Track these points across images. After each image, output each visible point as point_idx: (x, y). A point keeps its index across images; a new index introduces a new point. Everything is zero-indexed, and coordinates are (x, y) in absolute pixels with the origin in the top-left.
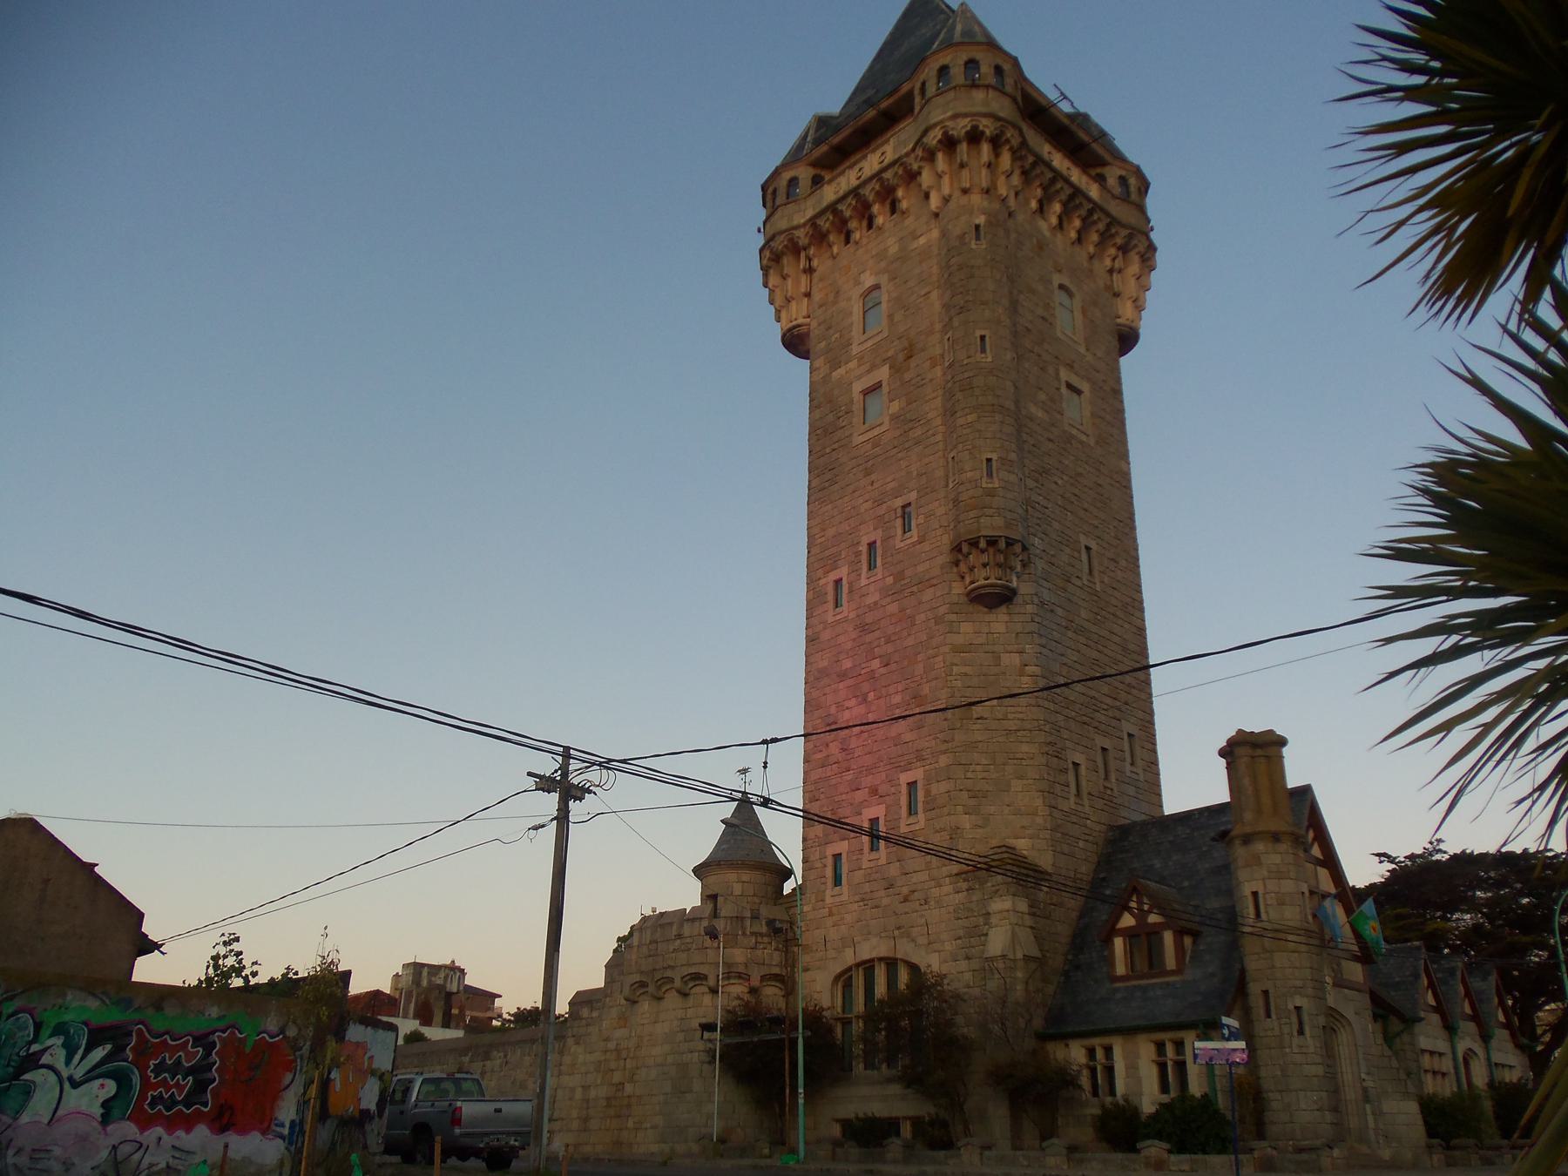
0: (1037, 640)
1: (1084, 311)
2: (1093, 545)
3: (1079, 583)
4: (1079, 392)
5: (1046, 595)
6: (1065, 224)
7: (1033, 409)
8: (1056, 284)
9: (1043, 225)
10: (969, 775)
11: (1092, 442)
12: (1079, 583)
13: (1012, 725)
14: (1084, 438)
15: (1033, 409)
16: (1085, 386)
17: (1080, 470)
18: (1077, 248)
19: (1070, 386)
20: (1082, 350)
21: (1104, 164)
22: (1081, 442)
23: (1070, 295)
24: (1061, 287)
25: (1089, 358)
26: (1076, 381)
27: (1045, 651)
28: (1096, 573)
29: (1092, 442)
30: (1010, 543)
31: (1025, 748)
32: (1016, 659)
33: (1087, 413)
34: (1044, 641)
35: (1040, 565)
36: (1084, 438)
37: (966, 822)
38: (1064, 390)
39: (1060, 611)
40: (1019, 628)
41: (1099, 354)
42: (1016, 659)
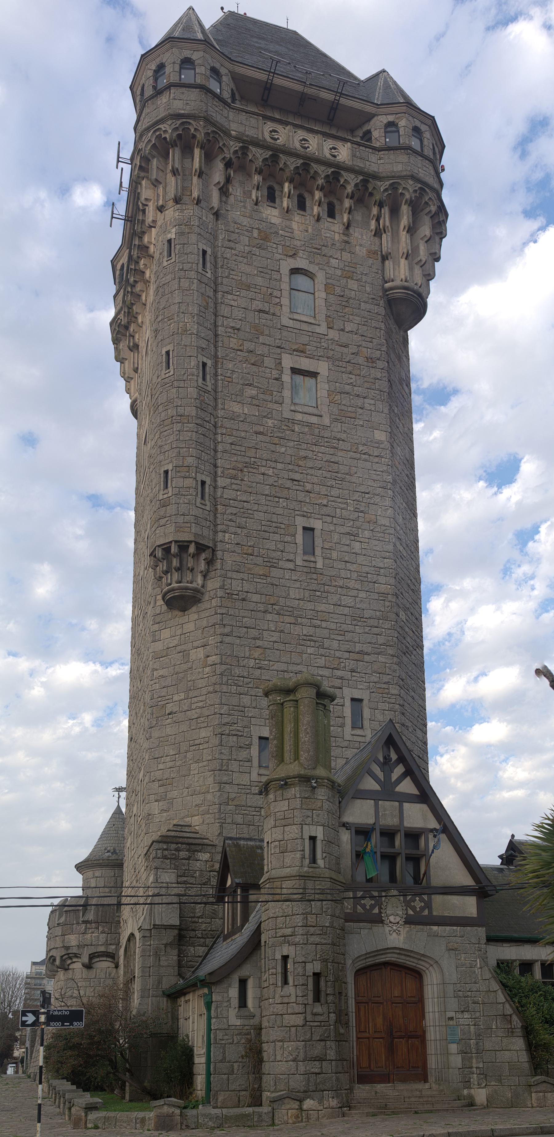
0: (219, 631)
1: (328, 288)
2: (317, 525)
3: (291, 565)
4: (314, 375)
5: (236, 586)
6: (308, 204)
7: (236, 408)
8: (285, 271)
9: (272, 214)
10: (161, 766)
11: (326, 421)
12: (291, 565)
13: (193, 714)
14: (314, 420)
15: (236, 408)
16: (322, 368)
17: (302, 453)
18: (327, 223)
19: (295, 371)
20: (322, 329)
21: (370, 117)
22: (310, 425)
23: (310, 275)
24: (295, 271)
25: (333, 334)
26: (305, 364)
27: (227, 639)
28: (318, 551)
29: (326, 421)
30: (183, 547)
31: (203, 733)
32: (201, 653)
33: (323, 393)
34: (227, 630)
35: (228, 559)
36: (314, 420)
37: (155, 808)
38: (286, 378)
39: (256, 598)
40: (204, 623)
41: (349, 327)
42: (201, 653)
